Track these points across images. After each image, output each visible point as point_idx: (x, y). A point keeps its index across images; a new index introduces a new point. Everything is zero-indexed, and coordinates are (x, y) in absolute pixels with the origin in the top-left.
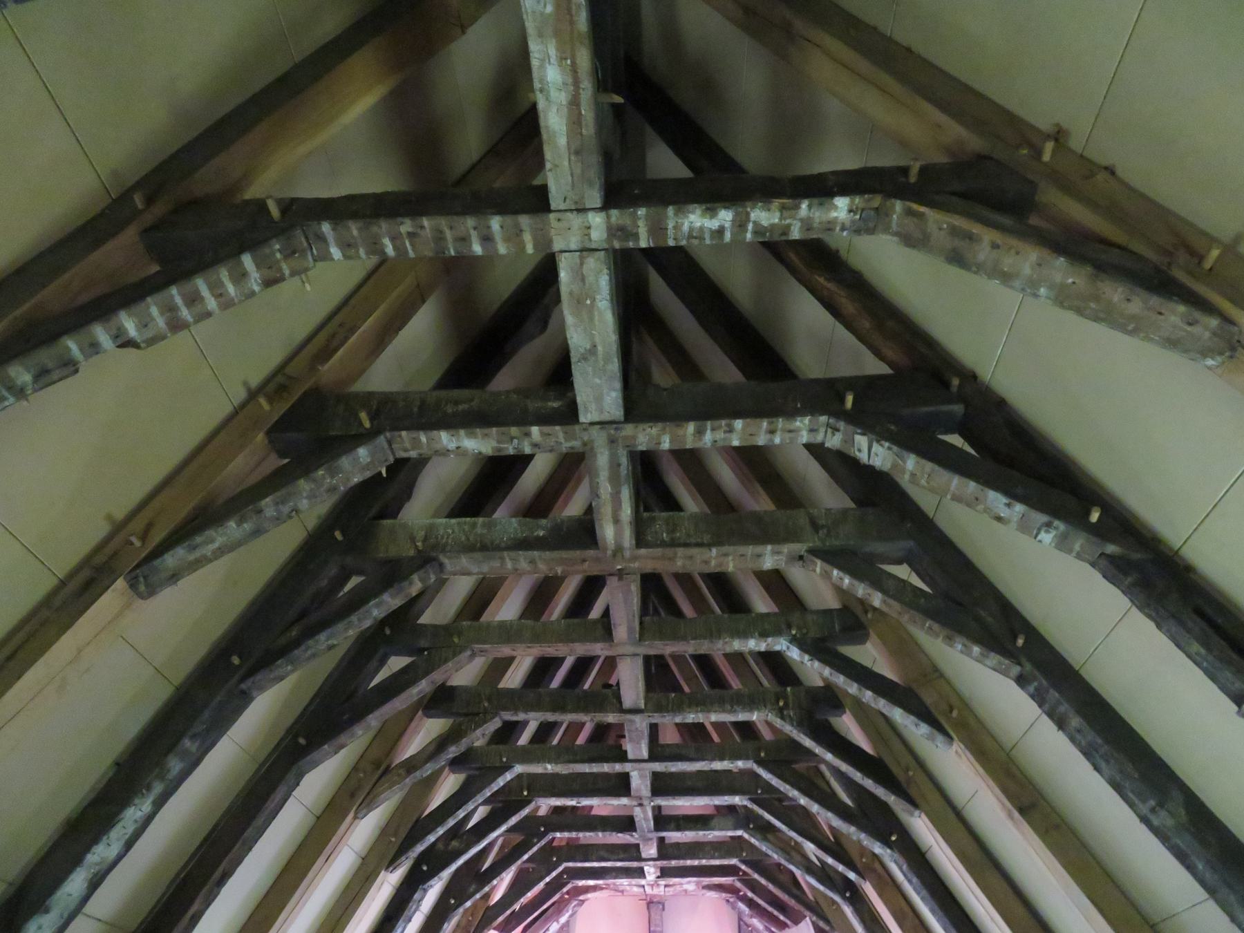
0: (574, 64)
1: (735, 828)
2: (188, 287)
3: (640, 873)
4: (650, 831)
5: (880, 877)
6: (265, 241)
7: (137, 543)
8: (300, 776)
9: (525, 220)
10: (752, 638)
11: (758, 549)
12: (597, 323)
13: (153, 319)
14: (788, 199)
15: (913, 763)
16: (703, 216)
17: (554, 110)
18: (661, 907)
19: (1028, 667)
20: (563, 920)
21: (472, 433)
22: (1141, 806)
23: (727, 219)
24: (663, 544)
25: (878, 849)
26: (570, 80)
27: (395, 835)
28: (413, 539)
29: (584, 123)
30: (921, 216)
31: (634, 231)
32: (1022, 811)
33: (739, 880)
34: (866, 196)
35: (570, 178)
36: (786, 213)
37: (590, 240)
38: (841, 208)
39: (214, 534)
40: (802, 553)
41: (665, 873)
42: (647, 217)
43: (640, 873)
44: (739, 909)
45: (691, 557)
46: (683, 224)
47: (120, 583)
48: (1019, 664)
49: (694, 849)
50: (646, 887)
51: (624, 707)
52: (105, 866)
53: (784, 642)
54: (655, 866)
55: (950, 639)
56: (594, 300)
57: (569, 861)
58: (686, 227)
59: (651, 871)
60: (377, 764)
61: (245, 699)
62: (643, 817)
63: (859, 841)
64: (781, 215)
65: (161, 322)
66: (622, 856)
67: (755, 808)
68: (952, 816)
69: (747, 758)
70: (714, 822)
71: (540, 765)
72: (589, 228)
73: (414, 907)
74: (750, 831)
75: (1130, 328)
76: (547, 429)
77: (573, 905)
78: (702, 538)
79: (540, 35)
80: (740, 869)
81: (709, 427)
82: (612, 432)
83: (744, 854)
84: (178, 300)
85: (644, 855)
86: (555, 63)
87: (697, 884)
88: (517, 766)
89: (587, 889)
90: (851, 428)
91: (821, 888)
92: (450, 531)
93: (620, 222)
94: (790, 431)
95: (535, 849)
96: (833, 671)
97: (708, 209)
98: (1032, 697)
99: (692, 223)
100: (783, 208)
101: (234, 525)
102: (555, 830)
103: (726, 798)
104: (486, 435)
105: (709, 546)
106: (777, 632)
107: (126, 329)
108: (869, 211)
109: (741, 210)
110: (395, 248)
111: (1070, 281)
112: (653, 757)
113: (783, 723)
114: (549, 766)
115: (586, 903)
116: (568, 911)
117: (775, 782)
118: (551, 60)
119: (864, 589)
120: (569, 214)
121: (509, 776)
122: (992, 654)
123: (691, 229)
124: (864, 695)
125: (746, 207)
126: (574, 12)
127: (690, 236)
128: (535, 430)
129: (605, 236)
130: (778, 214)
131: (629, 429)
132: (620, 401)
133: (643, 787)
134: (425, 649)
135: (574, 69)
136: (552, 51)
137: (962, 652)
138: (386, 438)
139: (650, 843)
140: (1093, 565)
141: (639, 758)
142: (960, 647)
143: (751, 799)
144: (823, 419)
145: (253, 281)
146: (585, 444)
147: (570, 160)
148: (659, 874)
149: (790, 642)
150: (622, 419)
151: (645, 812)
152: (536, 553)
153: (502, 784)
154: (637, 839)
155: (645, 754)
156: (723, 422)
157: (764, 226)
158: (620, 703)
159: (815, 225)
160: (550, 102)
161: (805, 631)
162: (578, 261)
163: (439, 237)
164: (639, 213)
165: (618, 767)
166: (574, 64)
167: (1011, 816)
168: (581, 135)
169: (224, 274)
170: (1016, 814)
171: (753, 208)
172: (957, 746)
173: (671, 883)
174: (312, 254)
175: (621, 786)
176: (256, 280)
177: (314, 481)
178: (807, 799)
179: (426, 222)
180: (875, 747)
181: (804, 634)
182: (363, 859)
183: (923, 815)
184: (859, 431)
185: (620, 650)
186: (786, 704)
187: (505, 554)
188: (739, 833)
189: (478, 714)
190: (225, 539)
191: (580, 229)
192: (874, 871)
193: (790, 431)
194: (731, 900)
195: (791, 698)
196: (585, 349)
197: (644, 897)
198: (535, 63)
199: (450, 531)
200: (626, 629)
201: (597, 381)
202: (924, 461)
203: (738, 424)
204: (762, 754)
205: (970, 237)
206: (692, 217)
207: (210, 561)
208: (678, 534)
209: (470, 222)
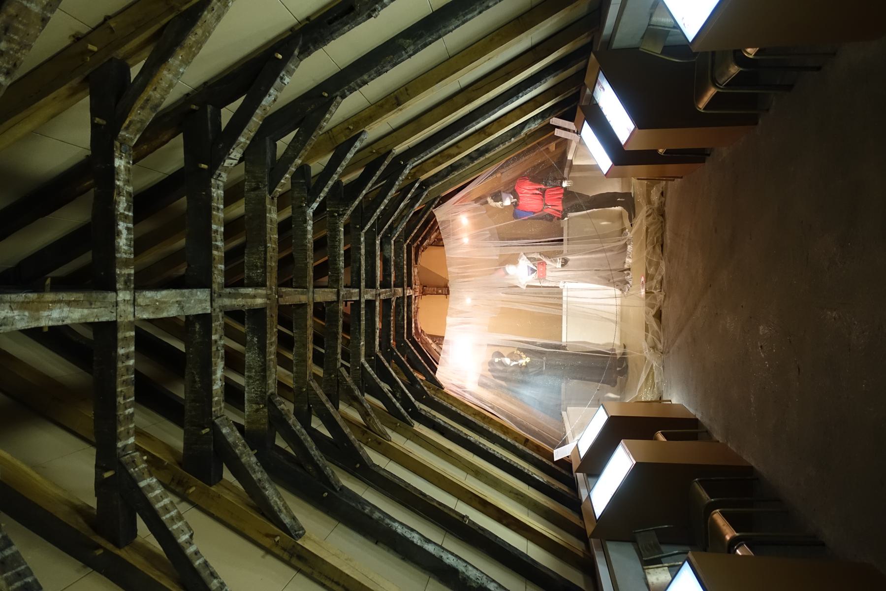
0: (51, 302)
2: (161, 512)
3: (410, 297)
4: (391, 291)
5: (418, 171)
6: (130, 476)
7: (278, 539)
8: (375, 465)
9: (120, 335)
10: (307, 228)
11: (268, 221)
12: (167, 300)
13: (179, 527)
14: (114, 191)
15: (369, 149)
17: (72, 314)
19: (338, 93)
21: (214, 372)
22: (404, 57)
24: (265, 272)
25: (407, 171)
27: (396, 424)
28: (257, 410)
29: (78, 299)
30: (131, 122)
32: (399, 105)
34: (115, 149)
35: (102, 309)
37: (130, 300)
39: (272, 501)
41: (410, 285)
42: (120, 269)
43: (410, 297)
45: (271, 258)
46: (124, 249)
47: (299, 542)
48: (336, 97)
49: (399, 268)
51: (336, 300)
52: (422, 539)
54: (407, 290)
55: (321, 127)
56: (157, 301)
57: (404, 337)
58: (126, 248)
59: (409, 292)
60: (364, 433)
61: (343, 488)
62: (384, 294)
63: (403, 180)
65: (180, 524)
66: (402, 308)
67: (382, 233)
68: (395, 133)
69: (360, 235)
70: (387, 255)
72: (124, 300)
74: (392, 236)
75: (208, 35)
76: (214, 332)
78: (262, 251)
79: (38, 319)
80: (408, 243)
81: (215, 243)
82: (216, 295)
83: (402, 240)
84: (168, 516)
85: (402, 295)
89: (416, 328)
90: (220, 168)
91: (421, 201)
92: (253, 390)
93: (122, 283)
94: (218, 199)
95: (399, 354)
96: (326, 187)
97: (118, 235)
98: (351, 93)
100: (119, 194)
101: (267, 492)
102: (390, 343)
103: (377, 248)
104: (215, 364)
105: (266, 247)
107: (186, 539)
108: (122, 148)
109: (119, 217)
110: (130, 408)
111: (180, 57)
112: (359, 287)
113: (346, 214)
114: (362, 343)
115: (422, 329)
116: (426, 339)
117: (372, 221)
118: (50, 314)
119: (292, 167)
120: (118, 311)
121: (367, 365)
122: (330, 109)
123: (127, 245)
126: (29, 300)
128: (214, 337)
129: (128, 292)
130: (121, 197)
131: (215, 286)
132: (202, 290)
133: (371, 293)
134: (309, 406)
135: (53, 302)
136: (46, 313)
137: (327, 123)
138: (215, 419)
139: (396, 291)
140: (301, 60)
141: (358, 294)
142: (325, 123)
144: (213, 181)
145: (151, 482)
147: (94, 308)
150: (210, 289)
151: (382, 293)
152: (268, 342)
155: (357, 290)
156: (213, 235)
157: (127, 206)
158: (334, 301)
159: (127, 178)
160: (68, 317)
161: (303, 199)
162: (139, 307)
163: (125, 382)
165: (363, 306)
166: (51, 302)
167: (401, 110)
168: (83, 301)
169: (151, 495)
171: (119, 211)
172: (366, 129)
174: (132, 453)
175: (370, 304)
176: (151, 480)
177: (241, 454)
179: (119, 389)
180: (361, 168)
181: (305, 199)
182: (408, 439)
183: (395, 148)
184: (222, 163)
185: (311, 299)
186: (336, 212)
187: (267, 359)
188: (393, 242)
189: (338, 380)
190: (274, 496)
191: (125, 305)
192: (415, 173)
193: (218, 199)
195: (333, 209)
196: (178, 307)
199: (253, 390)
200: (302, 296)
201: (193, 301)
202: (243, 133)
203: (214, 227)
204: (358, 226)
205: (147, 100)
206: (121, 244)
207: (285, 503)
209: (120, 365)
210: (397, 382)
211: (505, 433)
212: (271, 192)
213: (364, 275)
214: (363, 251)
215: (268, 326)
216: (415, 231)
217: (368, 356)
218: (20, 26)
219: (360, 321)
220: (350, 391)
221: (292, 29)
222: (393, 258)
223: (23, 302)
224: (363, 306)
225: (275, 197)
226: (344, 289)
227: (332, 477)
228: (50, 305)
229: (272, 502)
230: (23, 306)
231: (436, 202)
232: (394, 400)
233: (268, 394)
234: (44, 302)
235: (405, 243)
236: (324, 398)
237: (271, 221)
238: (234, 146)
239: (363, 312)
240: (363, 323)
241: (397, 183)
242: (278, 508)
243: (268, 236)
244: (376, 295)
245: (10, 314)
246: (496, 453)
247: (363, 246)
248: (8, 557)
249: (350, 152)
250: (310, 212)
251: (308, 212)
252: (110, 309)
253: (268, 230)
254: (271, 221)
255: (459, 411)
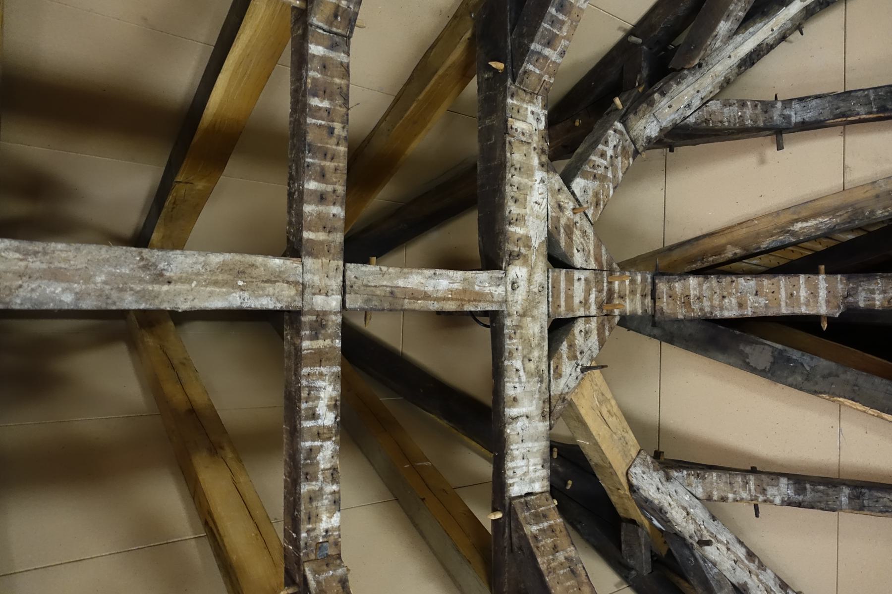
0: (449, 299)
9: (339, 237)
12: (209, 289)
16: (331, 398)
23: (325, 421)
26: (439, 295)
29: (412, 301)
31: (320, 336)
35: (373, 284)
36: (328, 473)
38: (331, 522)
42: (333, 348)
46: (324, 380)
56: (242, 289)
58: (320, 383)
64: (327, 470)
72: (327, 295)
79: (465, 280)
86: (450, 287)
99: (325, 389)
109: (334, 432)
118: (451, 285)
123: (318, 389)
125: (336, 436)
126: (474, 303)
127: (310, 388)
129: (318, 309)
130: (328, 466)
135: (445, 299)
136: (456, 286)
147: (387, 286)
159: (314, 504)
162: (291, 279)
164: (337, 341)
166: (449, 299)
168: (405, 298)
171: (334, 442)
174: (321, 28)
191: (326, 286)
198: (451, 273)
206: (330, 389)
218: (569, 584)
223: (480, 301)
228: (450, 296)
230: (480, 297)
234: (457, 300)
245: (493, 288)
248: (542, 44)
252: (359, 283)
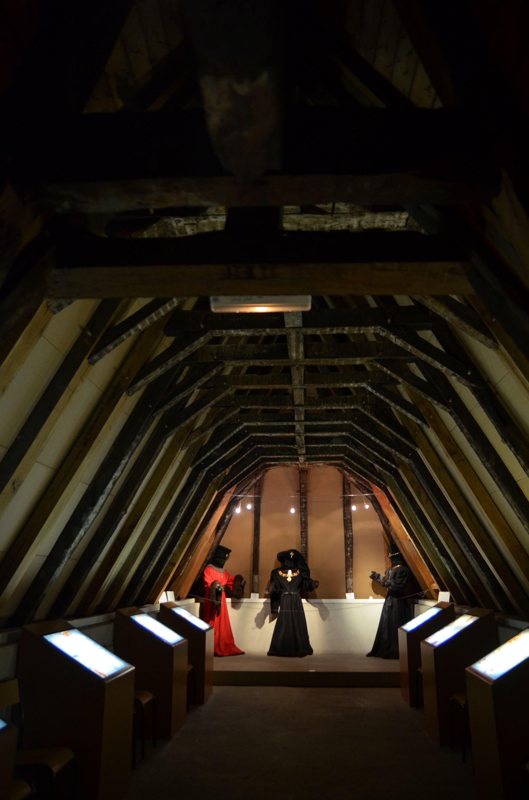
1: (343, 443)
3: (297, 460)
4: (302, 444)
7: (127, 378)
10: (352, 383)
11: (354, 359)
18: (306, 472)
19: (452, 410)
20: (258, 478)
22: (482, 459)
25: (403, 458)
33: (344, 462)
40: (372, 360)
41: (307, 460)
43: (297, 460)
44: (344, 473)
45: (327, 361)
47: (125, 393)
48: (450, 408)
50: (299, 465)
52: (116, 479)
53: (365, 385)
54: (304, 457)
57: (263, 455)
59: (302, 459)
62: (300, 439)
66: (288, 453)
67: (352, 437)
68: (431, 449)
69: (349, 420)
71: (255, 423)
73: (199, 479)
76: (272, 329)
77: (263, 472)
83: (347, 452)
85: (299, 453)
87: (324, 463)
88: (245, 423)
90: (389, 332)
92: (227, 350)
94: (366, 330)
95: (249, 452)
98: (454, 419)
102: (258, 444)
103: (339, 433)
105: (334, 358)
106: (363, 381)
112: (306, 420)
113: (364, 411)
114: (259, 423)
115: (269, 471)
116: (260, 474)
117: (361, 430)
121: (241, 427)
122: (440, 404)
124: (397, 407)
131: (304, 330)
132: (302, 322)
133: (301, 430)
134: (212, 387)
139: (302, 448)
140: (469, 387)
141: (300, 420)
143: (350, 434)
144: (379, 327)
146: (287, 333)
148: (305, 459)
149: (368, 385)
151: (301, 438)
152: (263, 360)
153: (238, 430)
154: (297, 447)
155: (303, 418)
158: (294, 403)
161: (374, 380)
165: (290, 423)
170: (449, 456)
173: (311, 463)
175: (292, 429)
178: (375, 438)
180: (403, 423)
183: (419, 449)
184: (392, 333)
186: (366, 404)
188: (345, 445)
193: (366, 330)
194: (340, 469)
195: (368, 400)
197: (298, 468)
199: (227, 350)
201: (293, 317)
202: (414, 348)
203: (347, 328)
204: (356, 419)
208: (322, 353)
210: (226, 452)
211: (180, 545)
212: (376, 360)
213: (316, 424)
214: (336, 423)
215: (275, 360)
216: (356, 464)
217: (247, 427)
219: (278, 421)
220: (221, 416)
221: (489, 381)
222: (331, 446)
224: (290, 423)
225: (373, 363)
226: (304, 410)
227: (163, 410)
229: (152, 373)
231: (381, 482)
232: (212, 451)
233: (224, 362)
235: (344, 455)
236: (218, 399)
237: (354, 361)
238: (404, 342)
239: (285, 424)
240: (276, 424)
241: (393, 450)
242: (148, 378)
243: (343, 359)
244: (299, 433)
246: (167, 536)
247: (339, 422)
249: (412, 416)
250: (364, 385)
251: (364, 384)
253: (347, 359)
254: (354, 361)
255: (199, 505)
